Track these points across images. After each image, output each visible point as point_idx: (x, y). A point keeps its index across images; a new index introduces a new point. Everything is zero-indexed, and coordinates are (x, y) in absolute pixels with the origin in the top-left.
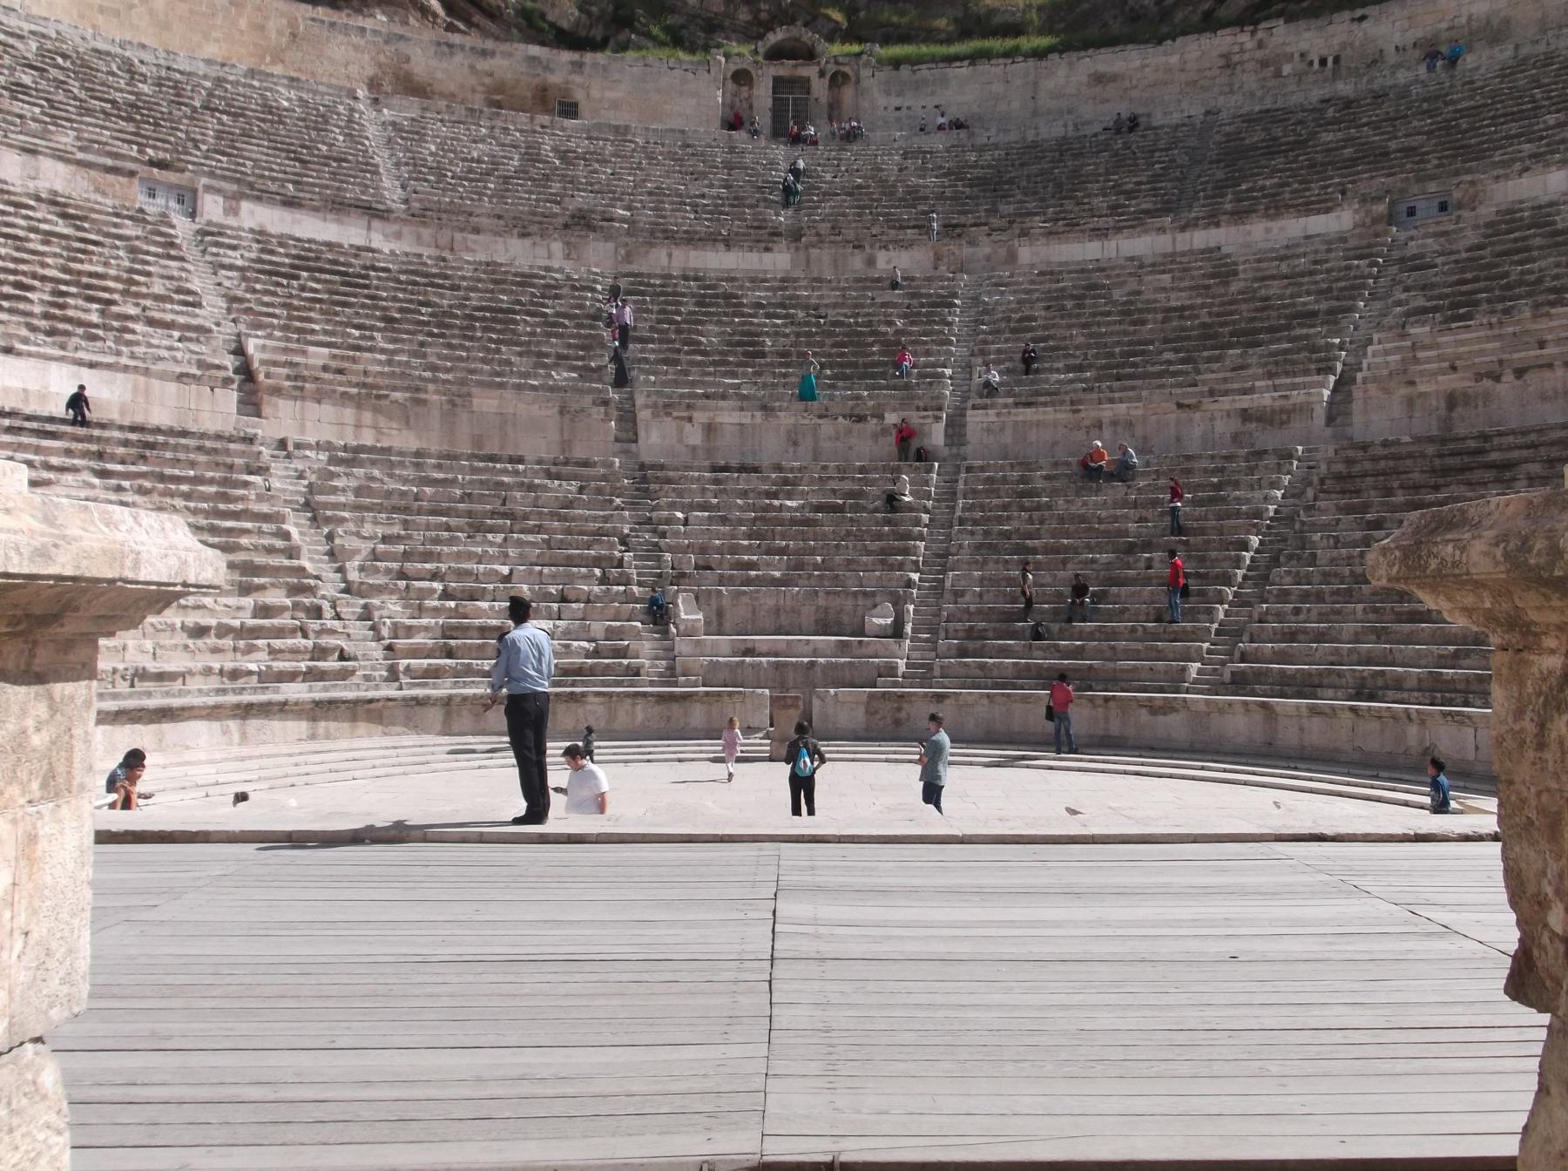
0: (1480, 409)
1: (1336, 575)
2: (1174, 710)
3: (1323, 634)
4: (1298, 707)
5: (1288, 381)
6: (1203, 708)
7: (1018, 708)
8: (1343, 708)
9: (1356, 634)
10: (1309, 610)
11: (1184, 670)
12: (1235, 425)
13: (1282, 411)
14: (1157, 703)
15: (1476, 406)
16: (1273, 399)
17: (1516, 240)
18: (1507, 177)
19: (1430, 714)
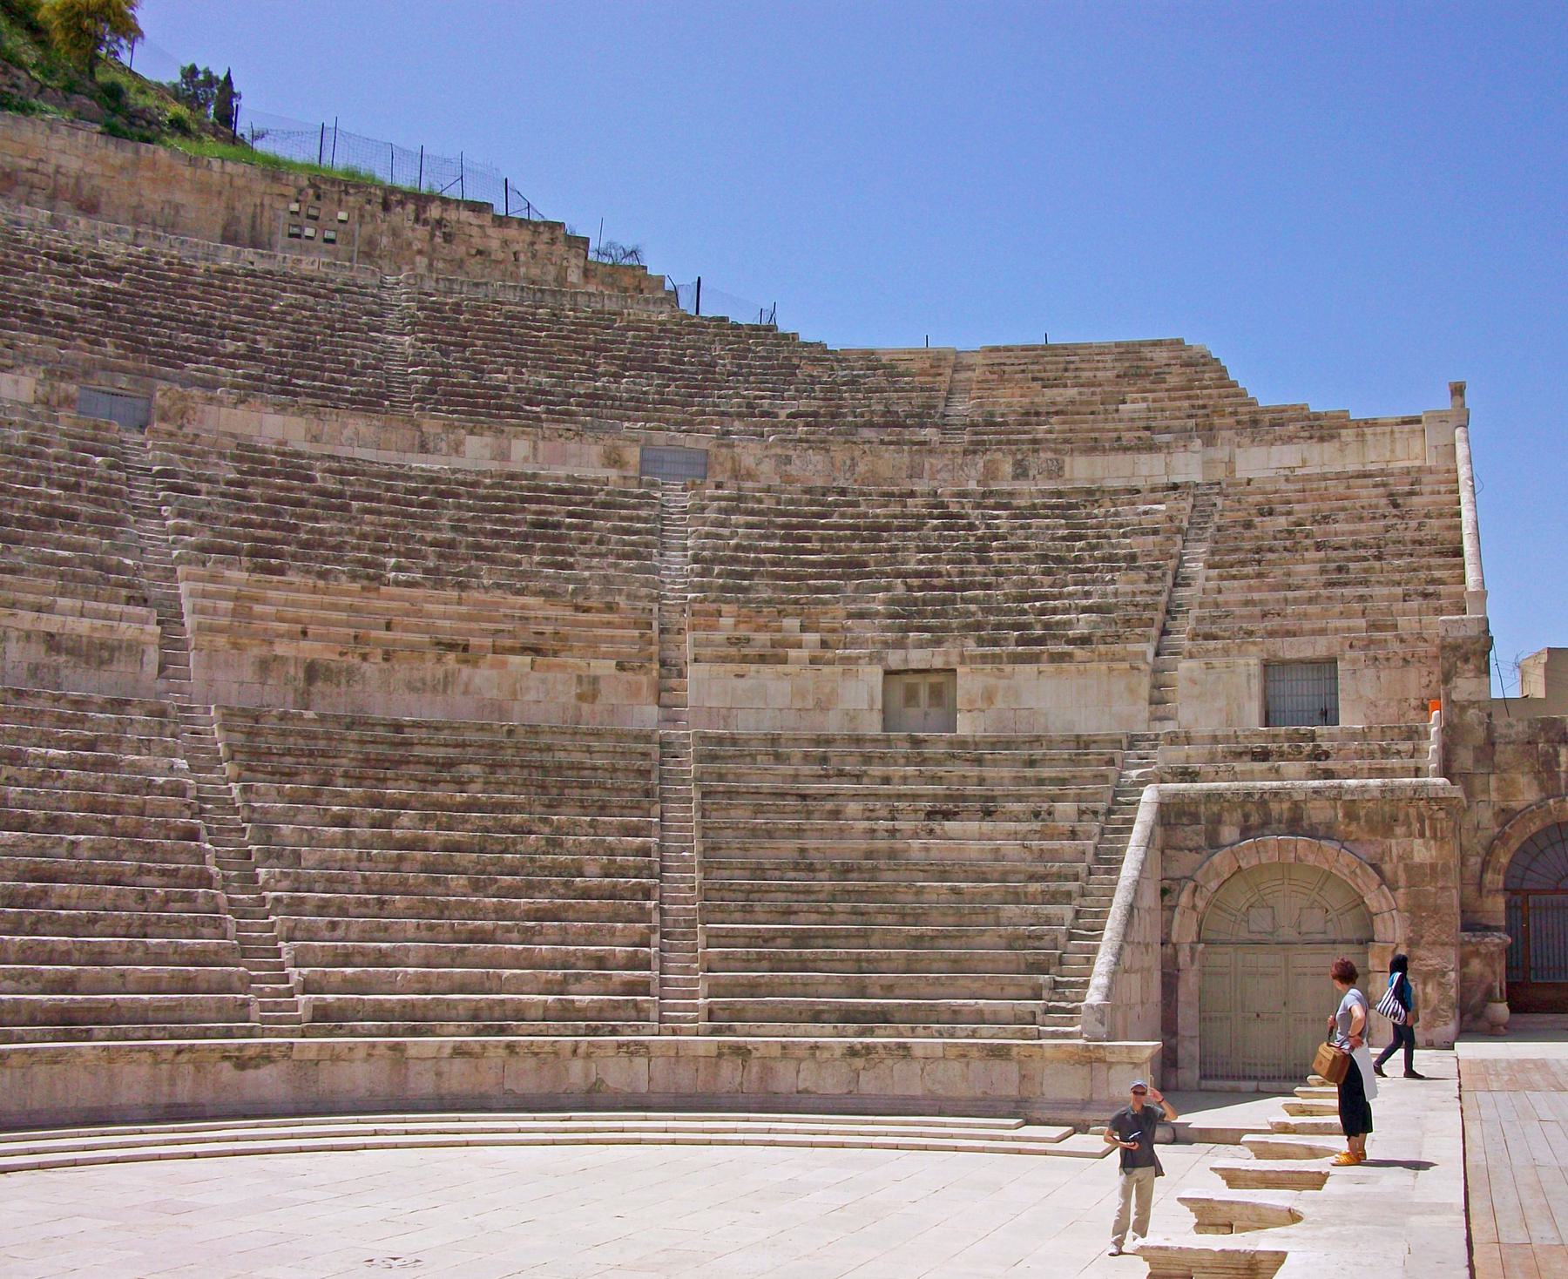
0: (343, 688)
1: (344, 881)
2: (269, 1059)
3: (347, 955)
4: (441, 1046)
5: (103, 606)
6: (312, 1055)
7: (41, 1072)
8: (497, 1045)
9: (427, 956)
10: (348, 925)
11: (245, 1004)
12: (37, 653)
13: (103, 646)
14: (248, 1053)
15: (338, 685)
16: (94, 629)
17: (281, 488)
18: (221, 403)
19: (599, 1046)
